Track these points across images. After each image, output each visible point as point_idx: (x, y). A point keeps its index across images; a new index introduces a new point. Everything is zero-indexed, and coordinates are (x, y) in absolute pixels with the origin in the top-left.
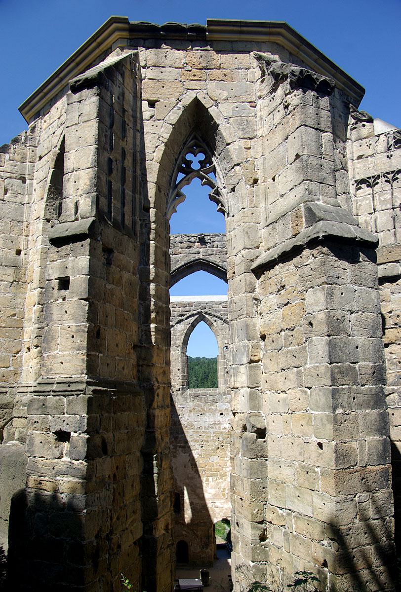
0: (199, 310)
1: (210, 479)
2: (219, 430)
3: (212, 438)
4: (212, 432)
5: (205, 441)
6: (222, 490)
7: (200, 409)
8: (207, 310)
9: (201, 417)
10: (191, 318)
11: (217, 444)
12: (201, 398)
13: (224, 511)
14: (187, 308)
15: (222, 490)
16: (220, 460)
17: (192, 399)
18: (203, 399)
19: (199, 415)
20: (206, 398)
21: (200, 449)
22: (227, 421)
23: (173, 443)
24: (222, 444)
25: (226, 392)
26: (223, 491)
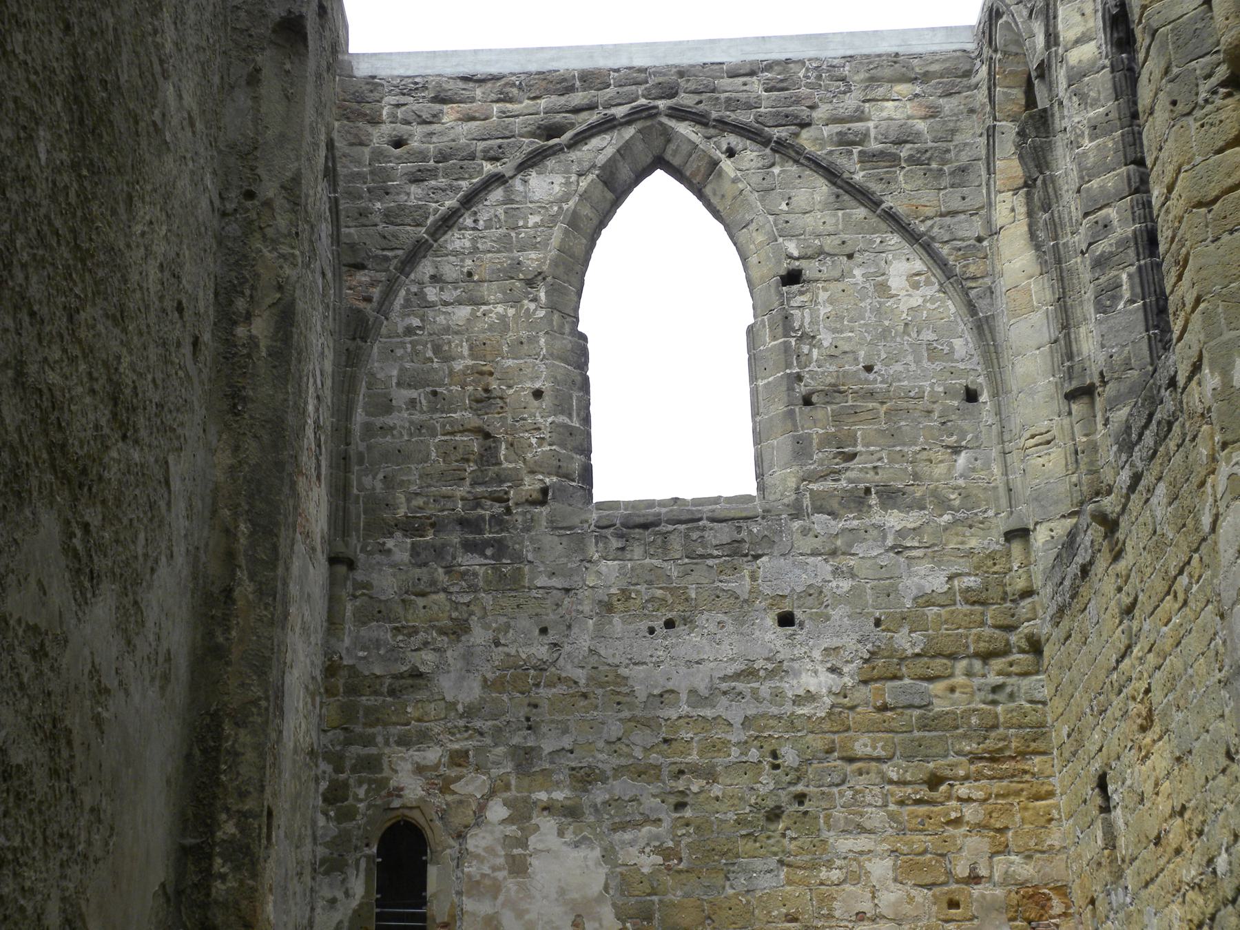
0: (643, 101)
2: (774, 710)
3: (735, 752)
4: (737, 720)
5: (696, 771)
7: (659, 593)
8: (686, 100)
9: (664, 639)
10: (595, 142)
12: (665, 535)
14: (578, 98)
16: (790, 882)
17: (615, 543)
18: (676, 544)
19: (659, 624)
20: (695, 535)
21: (668, 817)
22: (817, 654)
23: (507, 787)
24: (800, 788)
25: (807, 502)
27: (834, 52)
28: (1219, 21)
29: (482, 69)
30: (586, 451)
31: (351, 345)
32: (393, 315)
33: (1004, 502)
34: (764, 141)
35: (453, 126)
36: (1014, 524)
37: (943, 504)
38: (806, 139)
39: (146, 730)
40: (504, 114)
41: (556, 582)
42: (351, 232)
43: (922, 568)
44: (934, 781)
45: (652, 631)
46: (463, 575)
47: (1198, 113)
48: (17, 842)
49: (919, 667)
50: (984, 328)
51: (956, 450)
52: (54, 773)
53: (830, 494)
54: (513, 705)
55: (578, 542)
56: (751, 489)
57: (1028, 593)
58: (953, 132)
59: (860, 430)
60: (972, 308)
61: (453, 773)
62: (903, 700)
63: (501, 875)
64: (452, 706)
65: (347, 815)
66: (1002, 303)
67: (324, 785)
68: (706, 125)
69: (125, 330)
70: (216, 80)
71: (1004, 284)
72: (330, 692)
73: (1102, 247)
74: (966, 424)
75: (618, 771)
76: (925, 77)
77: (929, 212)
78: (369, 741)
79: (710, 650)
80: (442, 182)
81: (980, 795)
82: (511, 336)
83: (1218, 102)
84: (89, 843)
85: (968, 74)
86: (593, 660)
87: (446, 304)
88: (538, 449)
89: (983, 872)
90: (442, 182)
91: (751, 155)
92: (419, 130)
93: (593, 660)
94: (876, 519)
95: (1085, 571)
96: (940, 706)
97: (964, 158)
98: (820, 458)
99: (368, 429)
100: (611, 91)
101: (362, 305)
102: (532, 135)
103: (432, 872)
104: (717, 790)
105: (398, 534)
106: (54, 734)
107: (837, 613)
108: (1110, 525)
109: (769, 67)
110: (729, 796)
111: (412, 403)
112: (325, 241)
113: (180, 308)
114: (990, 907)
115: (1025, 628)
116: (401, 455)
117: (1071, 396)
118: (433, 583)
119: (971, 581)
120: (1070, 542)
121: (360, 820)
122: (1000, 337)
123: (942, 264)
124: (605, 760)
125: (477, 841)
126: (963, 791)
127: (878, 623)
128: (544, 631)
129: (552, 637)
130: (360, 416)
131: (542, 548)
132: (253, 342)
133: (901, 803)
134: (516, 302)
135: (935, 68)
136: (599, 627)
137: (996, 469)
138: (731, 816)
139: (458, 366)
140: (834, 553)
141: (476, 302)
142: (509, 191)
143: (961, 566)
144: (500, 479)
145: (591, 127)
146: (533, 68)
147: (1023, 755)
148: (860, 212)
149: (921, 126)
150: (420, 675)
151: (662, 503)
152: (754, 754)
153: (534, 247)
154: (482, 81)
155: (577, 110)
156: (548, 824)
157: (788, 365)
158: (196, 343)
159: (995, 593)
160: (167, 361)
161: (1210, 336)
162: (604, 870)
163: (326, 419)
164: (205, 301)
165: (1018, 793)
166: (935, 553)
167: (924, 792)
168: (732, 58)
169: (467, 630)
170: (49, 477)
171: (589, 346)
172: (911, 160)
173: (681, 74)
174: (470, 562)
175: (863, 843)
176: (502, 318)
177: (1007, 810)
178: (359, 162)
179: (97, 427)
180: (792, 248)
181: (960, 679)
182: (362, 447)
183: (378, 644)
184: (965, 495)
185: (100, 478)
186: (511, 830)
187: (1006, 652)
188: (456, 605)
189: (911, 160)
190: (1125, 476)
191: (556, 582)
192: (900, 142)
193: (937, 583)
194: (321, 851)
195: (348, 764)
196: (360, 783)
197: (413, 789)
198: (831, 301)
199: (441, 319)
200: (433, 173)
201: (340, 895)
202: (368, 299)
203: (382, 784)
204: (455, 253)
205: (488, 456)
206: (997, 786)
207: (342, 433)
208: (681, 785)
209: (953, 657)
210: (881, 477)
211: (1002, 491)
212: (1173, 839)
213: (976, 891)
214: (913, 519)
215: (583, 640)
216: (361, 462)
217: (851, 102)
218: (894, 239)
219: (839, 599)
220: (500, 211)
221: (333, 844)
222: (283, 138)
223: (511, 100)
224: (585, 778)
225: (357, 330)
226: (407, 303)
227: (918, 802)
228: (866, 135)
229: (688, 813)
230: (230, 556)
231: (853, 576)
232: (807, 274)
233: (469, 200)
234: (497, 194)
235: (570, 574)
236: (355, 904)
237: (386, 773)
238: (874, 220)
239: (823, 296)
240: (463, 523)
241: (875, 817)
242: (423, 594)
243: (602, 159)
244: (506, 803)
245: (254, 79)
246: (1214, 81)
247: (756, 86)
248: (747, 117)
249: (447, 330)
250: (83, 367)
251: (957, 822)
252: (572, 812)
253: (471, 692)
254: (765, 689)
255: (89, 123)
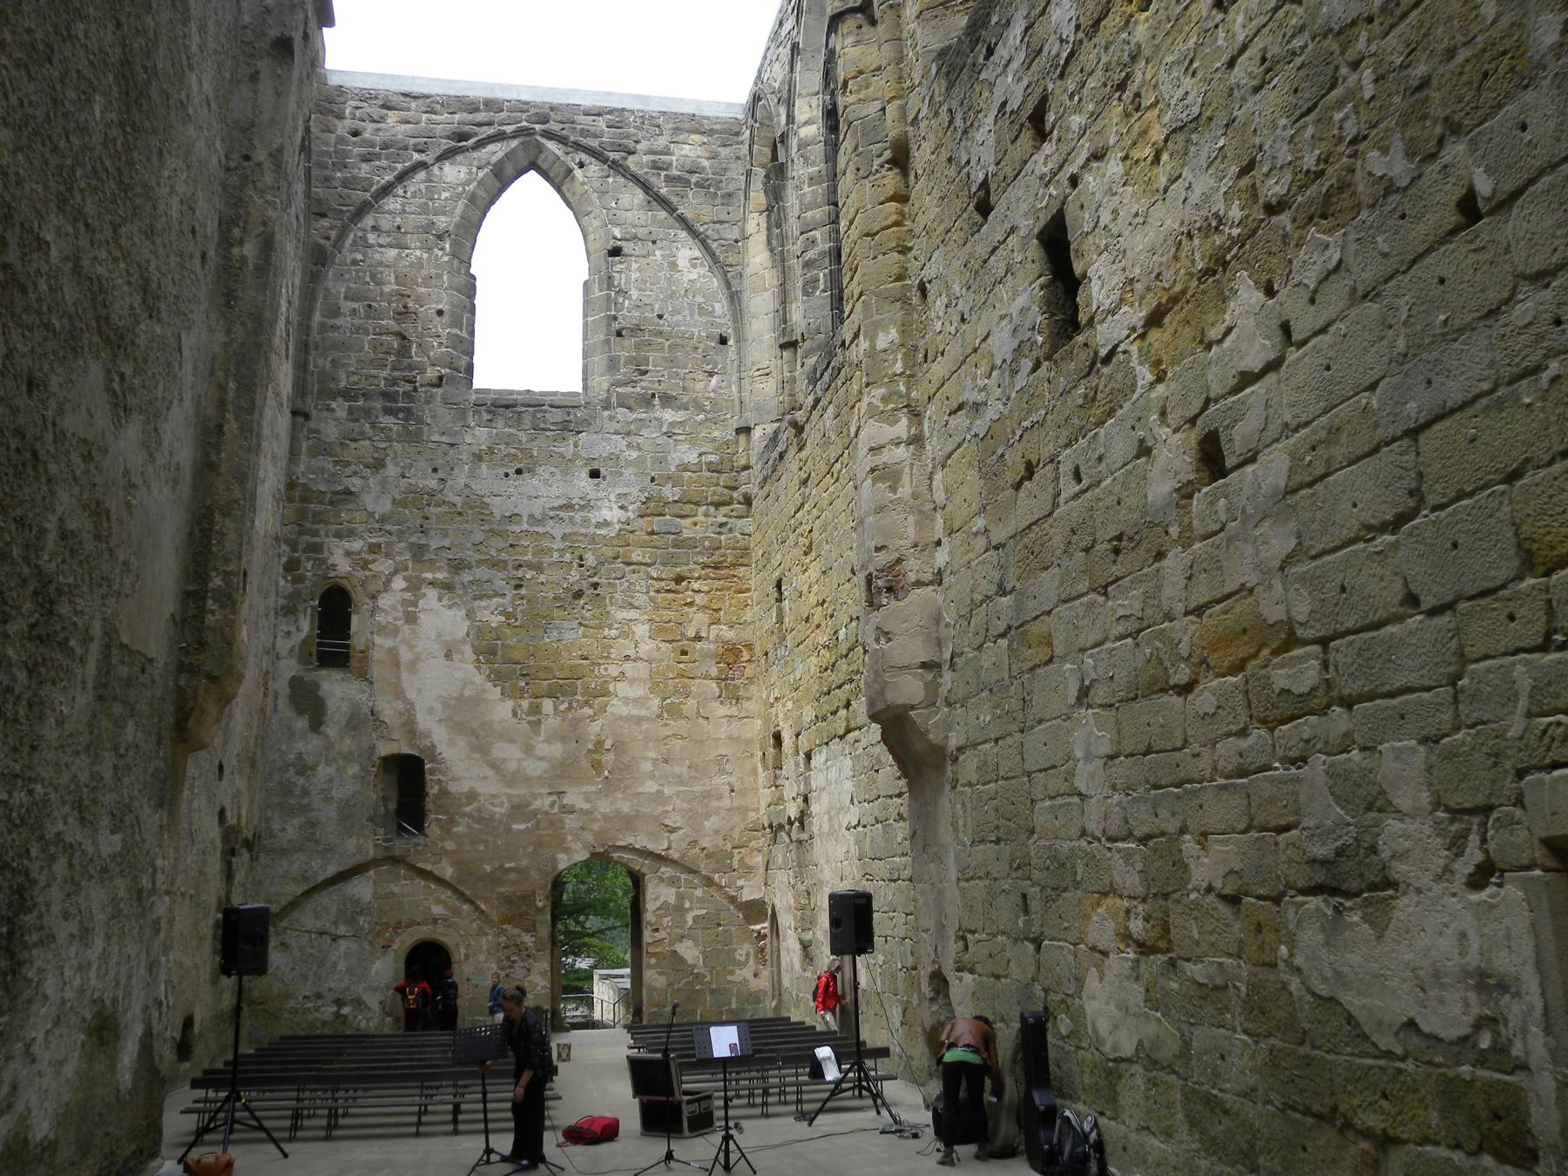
1: (547, 705)
2: (583, 530)
3: (556, 555)
4: (559, 536)
5: (530, 566)
6: (591, 747)
8: (553, 126)
10: (491, 147)
11: (574, 575)
13: (596, 827)
14: (481, 116)
15: (591, 747)
17: (486, 416)
18: (527, 421)
19: (511, 471)
22: (613, 497)
23: (406, 569)
24: (595, 579)
25: (614, 399)
26: (594, 752)
27: (654, 108)
28: (889, 123)
29: (417, 90)
30: (471, 354)
31: (315, 269)
32: (344, 251)
33: (737, 409)
34: (605, 161)
35: (393, 125)
36: (742, 424)
37: (700, 408)
38: (631, 162)
39: (163, 515)
40: (430, 121)
41: (444, 439)
42: (318, 191)
43: (684, 447)
44: (679, 579)
45: (507, 475)
46: (383, 429)
47: (871, 178)
48: (71, 580)
49: (676, 509)
50: (734, 298)
51: (711, 374)
52: (97, 537)
53: (629, 395)
54: (412, 516)
55: (462, 414)
56: (578, 388)
57: (747, 467)
58: (726, 170)
59: (652, 356)
60: (728, 284)
61: (370, 557)
62: (664, 529)
63: (399, 623)
64: (371, 514)
65: (299, 579)
66: (747, 283)
67: (284, 560)
68: (566, 145)
69: (153, 243)
70: (228, 75)
71: (749, 271)
72: (290, 500)
73: (810, 255)
74: (718, 358)
75: (479, 563)
76: (711, 132)
77: (707, 219)
78: (315, 533)
79: (544, 490)
80: (384, 163)
81: (706, 588)
82: (424, 272)
83: (884, 172)
84: (122, 585)
85: (737, 134)
86: (467, 491)
87: (381, 246)
88: (438, 350)
89: (703, 634)
90: (384, 163)
91: (594, 168)
92: (370, 126)
93: (467, 491)
94: (657, 414)
95: (781, 456)
96: (686, 534)
97: (731, 188)
98: (625, 371)
99: (323, 326)
100: (504, 114)
101: (323, 242)
102: (448, 138)
103: (355, 619)
104: (542, 578)
105: (340, 399)
106: (98, 511)
107: (627, 472)
108: (799, 428)
109: (611, 112)
110: (551, 582)
111: (354, 311)
112: (300, 196)
113: (193, 231)
114: (705, 655)
115: (743, 489)
116: (344, 346)
117: (783, 347)
118: (362, 433)
119: (712, 458)
120: (774, 439)
121: (308, 583)
122: (744, 305)
123: (712, 254)
124: (471, 555)
125: (384, 601)
126: (696, 586)
127: (653, 480)
128: (435, 470)
129: (440, 475)
130: (317, 318)
131: (436, 416)
132: (243, 259)
133: (658, 591)
134: (430, 249)
135: (717, 127)
136: (472, 471)
137: (734, 388)
138: (551, 595)
139: (387, 289)
140: (628, 434)
141: (402, 247)
142: (429, 174)
143: (708, 448)
144: (411, 368)
145: (489, 137)
146: (452, 93)
147: (734, 566)
148: (663, 214)
149: (706, 163)
150: (351, 493)
151: (519, 393)
152: (568, 558)
153: (444, 214)
154: (416, 98)
155: (480, 125)
156: (432, 593)
157: (609, 309)
158: (204, 256)
159: (726, 466)
160: (183, 267)
161: (866, 317)
162: (468, 623)
163: (294, 318)
164: (211, 228)
165: (729, 588)
166: (692, 440)
167: (672, 585)
168: (587, 103)
169: (384, 466)
170: (96, 339)
171: (478, 284)
172: (698, 184)
173: (552, 109)
174: (387, 421)
175: (632, 614)
176: (419, 259)
177: (721, 599)
178: (327, 144)
179: (132, 308)
180: (617, 232)
181: (701, 518)
182: (318, 338)
183: (323, 471)
184: (714, 404)
185: (133, 343)
186: (408, 595)
187: (729, 504)
188: (377, 449)
189: (698, 184)
190: (811, 399)
191: (444, 439)
192: (691, 172)
193: (692, 457)
194: (281, 602)
195: (300, 547)
196: (308, 560)
197: (344, 566)
198: (639, 270)
199: (377, 256)
200: (378, 157)
201: (293, 630)
202: (328, 238)
203: (323, 561)
204: (390, 212)
205: (404, 351)
206: (717, 584)
207: (305, 327)
208: (520, 574)
209: (697, 504)
210: (662, 388)
211: (737, 402)
212: (816, 620)
213: (699, 645)
214: (680, 416)
215: (460, 478)
216: (316, 348)
217: (662, 142)
218: (683, 234)
219: (630, 463)
220: (423, 186)
221: (289, 597)
222: (272, 121)
223: (435, 113)
224: (458, 566)
225: (319, 259)
226: (355, 243)
227: (668, 591)
228: (670, 164)
229: (523, 591)
230: (222, 404)
231: (640, 449)
232: (625, 250)
233: (402, 177)
234: (422, 175)
235: (455, 434)
236: (303, 635)
237: (326, 554)
238: (671, 220)
239: (634, 266)
240: (384, 395)
241: (641, 599)
242: (355, 440)
243: (494, 159)
244: (404, 579)
245: (254, 77)
246: (882, 159)
247: (601, 123)
248: (594, 143)
249: (381, 264)
250: (122, 265)
251: (691, 604)
252: (448, 587)
253: (384, 506)
254: (578, 517)
255: (133, 95)
